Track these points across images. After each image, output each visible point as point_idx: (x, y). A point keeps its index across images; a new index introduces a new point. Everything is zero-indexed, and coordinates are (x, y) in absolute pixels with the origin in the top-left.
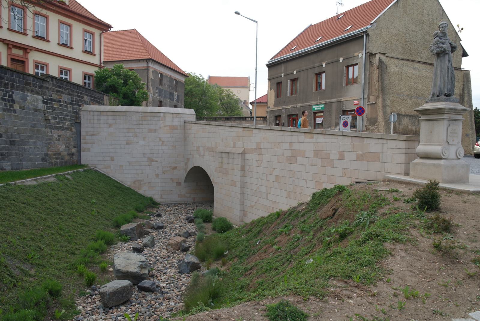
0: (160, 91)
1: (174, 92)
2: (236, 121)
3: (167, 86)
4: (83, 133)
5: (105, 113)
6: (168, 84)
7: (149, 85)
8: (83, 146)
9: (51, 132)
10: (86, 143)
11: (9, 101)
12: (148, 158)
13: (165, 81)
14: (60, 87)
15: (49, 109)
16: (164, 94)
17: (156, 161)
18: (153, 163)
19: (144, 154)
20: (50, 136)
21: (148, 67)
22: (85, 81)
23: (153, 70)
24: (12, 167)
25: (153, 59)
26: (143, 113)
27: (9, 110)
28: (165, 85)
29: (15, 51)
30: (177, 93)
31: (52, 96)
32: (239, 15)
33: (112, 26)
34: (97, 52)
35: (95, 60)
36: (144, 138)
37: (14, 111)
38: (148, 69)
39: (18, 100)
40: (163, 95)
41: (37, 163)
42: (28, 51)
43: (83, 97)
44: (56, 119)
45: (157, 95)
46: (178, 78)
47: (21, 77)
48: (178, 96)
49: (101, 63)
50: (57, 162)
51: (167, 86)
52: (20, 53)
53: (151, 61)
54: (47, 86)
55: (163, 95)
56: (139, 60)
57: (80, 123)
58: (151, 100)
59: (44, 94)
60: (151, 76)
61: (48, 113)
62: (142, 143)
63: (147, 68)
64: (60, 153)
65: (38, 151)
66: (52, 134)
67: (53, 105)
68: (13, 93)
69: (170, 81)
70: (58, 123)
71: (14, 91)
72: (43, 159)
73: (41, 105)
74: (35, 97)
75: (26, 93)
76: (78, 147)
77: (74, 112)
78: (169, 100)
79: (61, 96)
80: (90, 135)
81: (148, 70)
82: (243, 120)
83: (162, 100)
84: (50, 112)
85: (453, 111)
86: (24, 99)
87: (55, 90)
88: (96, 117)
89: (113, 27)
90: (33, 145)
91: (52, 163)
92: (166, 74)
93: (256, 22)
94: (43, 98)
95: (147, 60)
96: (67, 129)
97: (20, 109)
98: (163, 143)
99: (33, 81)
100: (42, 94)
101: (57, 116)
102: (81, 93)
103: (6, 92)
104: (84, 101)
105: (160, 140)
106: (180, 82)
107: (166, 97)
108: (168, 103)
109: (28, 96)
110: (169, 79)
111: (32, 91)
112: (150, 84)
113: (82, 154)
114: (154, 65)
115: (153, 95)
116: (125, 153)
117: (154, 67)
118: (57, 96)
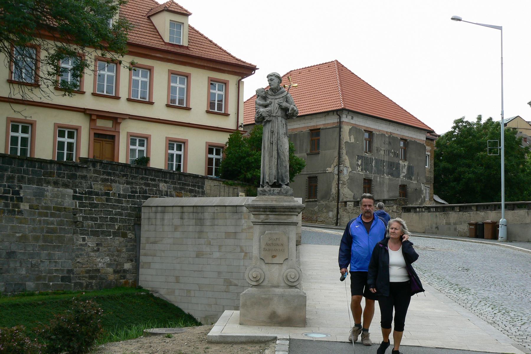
0: (366, 164)
1: (401, 162)
2: (478, 212)
3: (382, 152)
4: (143, 240)
5: (170, 209)
6: (384, 148)
7: (341, 152)
8: (143, 259)
9: (84, 239)
10: (145, 255)
11: (12, 199)
12: (226, 280)
13: (376, 143)
14: (109, 174)
15: (85, 207)
16: (375, 166)
17: (236, 285)
18: (232, 288)
19: (219, 273)
20: (81, 245)
21: (340, 122)
22: (210, 156)
23: (351, 127)
24: (6, 288)
25: (347, 108)
26: (219, 208)
27: (12, 212)
28: (378, 150)
29: (100, 123)
30: (406, 163)
31: (91, 188)
32: (461, 21)
33: (257, 67)
34: (231, 109)
35: (229, 123)
36: (220, 246)
37: (20, 212)
38: (339, 126)
39: (28, 197)
40: (374, 168)
41: (51, 284)
42: (119, 121)
43: (157, 186)
44: (97, 221)
45: (359, 169)
46: (410, 135)
47: (37, 166)
48: (410, 168)
49: (238, 127)
50: (91, 283)
51: (382, 152)
52: (108, 124)
53: (345, 113)
54: (85, 173)
55: (374, 168)
56: (327, 113)
57: (140, 224)
58: (347, 178)
59: (77, 186)
60: (346, 137)
61: (82, 212)
62: (217, 255)
63: (339, 124)
64: (99, 270)
65: (55, 266)
66: (84, 243)
67: (93, 200)
68: (21, 188)
69: (390, 143)
70: (100, 226)
71: (23, 185)
72: (63, 279)
73: (69, 202)
74: (60, 191)
75: (44, 187)
76: (135, 260)
77: (134, 209)
78: (387, 177)
79: (111, 186)
80: (151, 243)
81: (340, 128)
82: (491, 210)
83: (372, 176)
84: (85, 210)
85: (261, 210)
86: (40, 195)
87: (99, 179)
88: (159, 216)
89: (258, 69)
90: (47, 258)
91: (81, 284)
92: (379, 131)
93: (500, 28)
94: (75, 192)
95: (338, 112)
96: (115, 234)
97: (30, 208)
98: (245, 256)
99: (57, 170)
100: (74, 187)
101: (98, 216)
102: (154, 180)
103: (9, 187)
104: (159, 190)
105: (242, 251)
106: (415, 143)
107: (380, 172)
108: (387, 181)
109: (47, 191)
110: (387, 139)
111: (56, 184)
112: (344, 151)
113: (141, 271)
114: (352, 118)
115: (350, 170)
116: (195, 271)
117: (353, 122)
118: (102, 187)
